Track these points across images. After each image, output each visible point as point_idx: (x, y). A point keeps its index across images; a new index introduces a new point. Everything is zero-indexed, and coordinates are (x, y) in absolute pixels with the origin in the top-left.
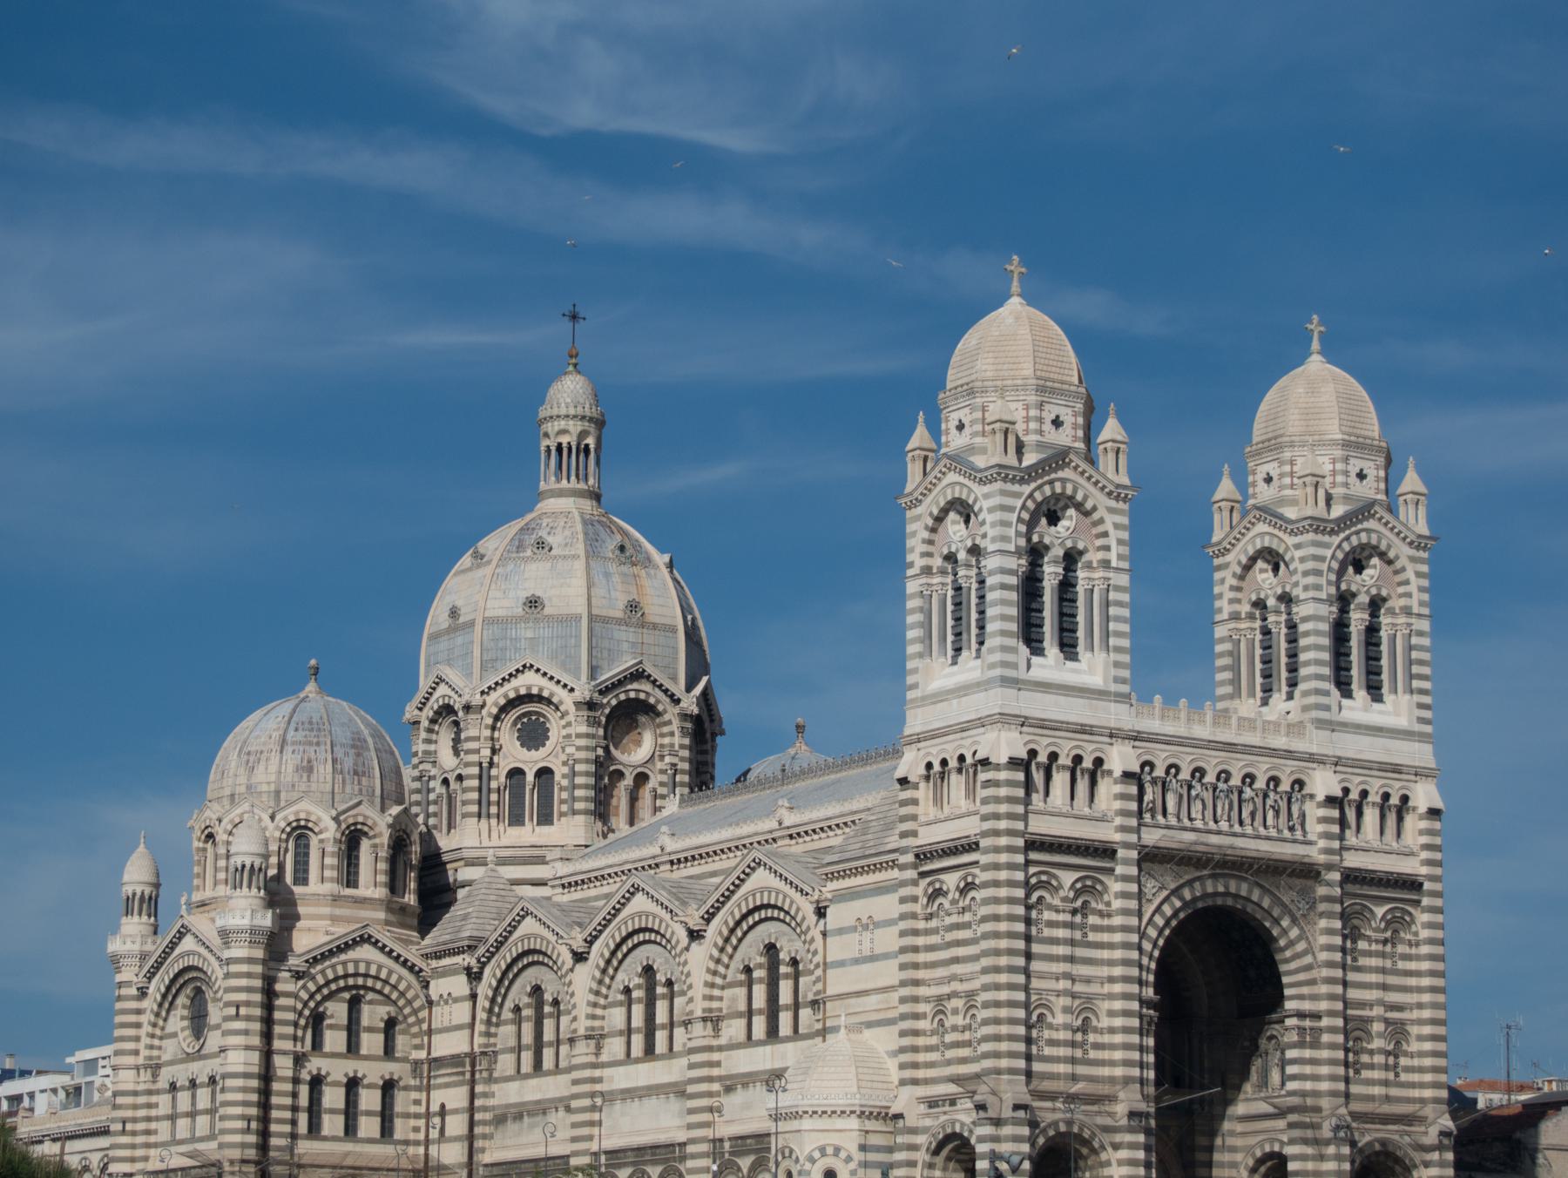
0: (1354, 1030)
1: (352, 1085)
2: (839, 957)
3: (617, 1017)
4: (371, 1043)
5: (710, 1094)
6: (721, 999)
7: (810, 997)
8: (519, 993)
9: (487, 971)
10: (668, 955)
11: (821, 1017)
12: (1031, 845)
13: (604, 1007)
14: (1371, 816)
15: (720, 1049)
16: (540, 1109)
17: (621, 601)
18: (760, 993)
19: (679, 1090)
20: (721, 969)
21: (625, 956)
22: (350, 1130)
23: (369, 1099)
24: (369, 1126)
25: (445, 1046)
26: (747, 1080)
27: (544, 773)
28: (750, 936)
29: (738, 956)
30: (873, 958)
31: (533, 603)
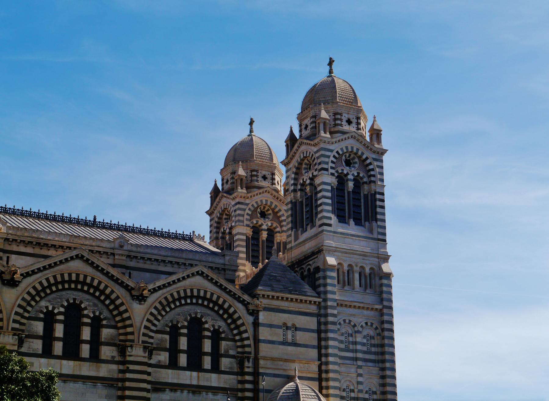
2: (270, 338)
3: (39, 327)
5: (148, 391)
6: (152, 337)
7: (232, 352)
10: (96, 301)
11: (250, 364)
13: (29, 318)
15: (150, 365)
18: (183, 343)
20: (156, 322)
21: (52, 292)
26: (175, 387)
28: (178, 310)
29: (167, 318)
30: (294, 344)
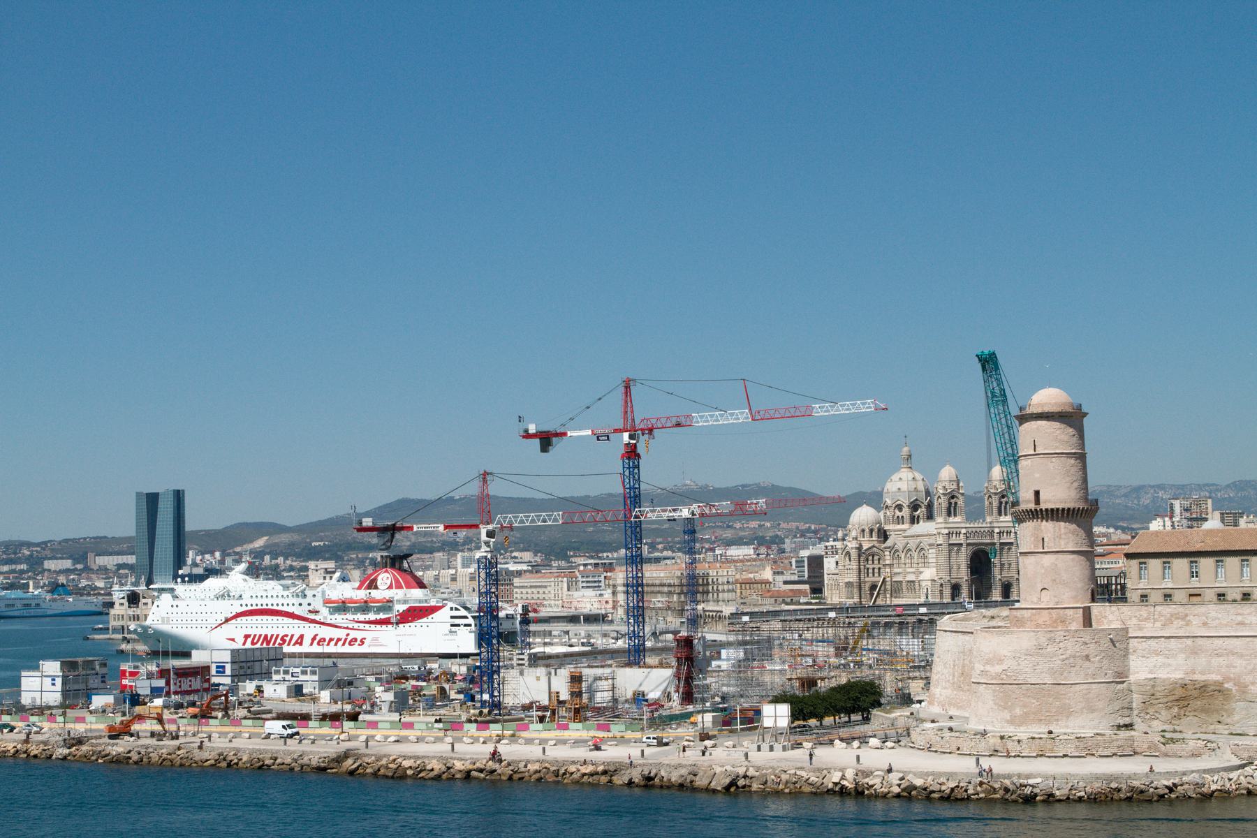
0: (1002, 565)
1: (874, 569)
4: (876, 562)
8: (896, 555)
9: (892, 552)
12: (950, 545)
14: (1005, 534)
16: (899, 573)
17: (914, 487)
19: (914, 573)
22: (874, 575)
23: (876, 571)
24: (876, 575)
25: (888, 562)
27: (902, 517)
31: (899, 489)
